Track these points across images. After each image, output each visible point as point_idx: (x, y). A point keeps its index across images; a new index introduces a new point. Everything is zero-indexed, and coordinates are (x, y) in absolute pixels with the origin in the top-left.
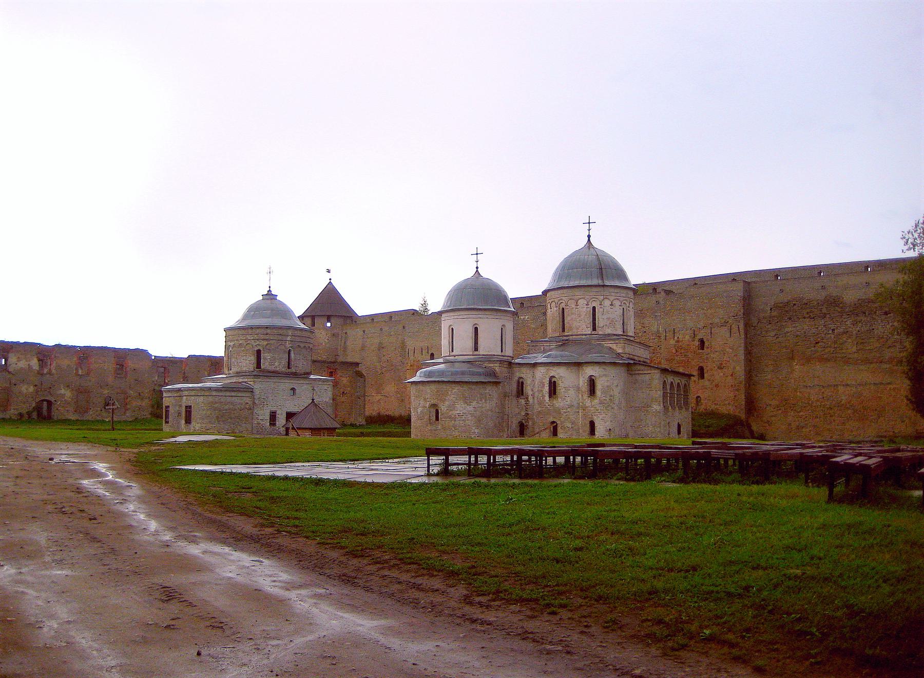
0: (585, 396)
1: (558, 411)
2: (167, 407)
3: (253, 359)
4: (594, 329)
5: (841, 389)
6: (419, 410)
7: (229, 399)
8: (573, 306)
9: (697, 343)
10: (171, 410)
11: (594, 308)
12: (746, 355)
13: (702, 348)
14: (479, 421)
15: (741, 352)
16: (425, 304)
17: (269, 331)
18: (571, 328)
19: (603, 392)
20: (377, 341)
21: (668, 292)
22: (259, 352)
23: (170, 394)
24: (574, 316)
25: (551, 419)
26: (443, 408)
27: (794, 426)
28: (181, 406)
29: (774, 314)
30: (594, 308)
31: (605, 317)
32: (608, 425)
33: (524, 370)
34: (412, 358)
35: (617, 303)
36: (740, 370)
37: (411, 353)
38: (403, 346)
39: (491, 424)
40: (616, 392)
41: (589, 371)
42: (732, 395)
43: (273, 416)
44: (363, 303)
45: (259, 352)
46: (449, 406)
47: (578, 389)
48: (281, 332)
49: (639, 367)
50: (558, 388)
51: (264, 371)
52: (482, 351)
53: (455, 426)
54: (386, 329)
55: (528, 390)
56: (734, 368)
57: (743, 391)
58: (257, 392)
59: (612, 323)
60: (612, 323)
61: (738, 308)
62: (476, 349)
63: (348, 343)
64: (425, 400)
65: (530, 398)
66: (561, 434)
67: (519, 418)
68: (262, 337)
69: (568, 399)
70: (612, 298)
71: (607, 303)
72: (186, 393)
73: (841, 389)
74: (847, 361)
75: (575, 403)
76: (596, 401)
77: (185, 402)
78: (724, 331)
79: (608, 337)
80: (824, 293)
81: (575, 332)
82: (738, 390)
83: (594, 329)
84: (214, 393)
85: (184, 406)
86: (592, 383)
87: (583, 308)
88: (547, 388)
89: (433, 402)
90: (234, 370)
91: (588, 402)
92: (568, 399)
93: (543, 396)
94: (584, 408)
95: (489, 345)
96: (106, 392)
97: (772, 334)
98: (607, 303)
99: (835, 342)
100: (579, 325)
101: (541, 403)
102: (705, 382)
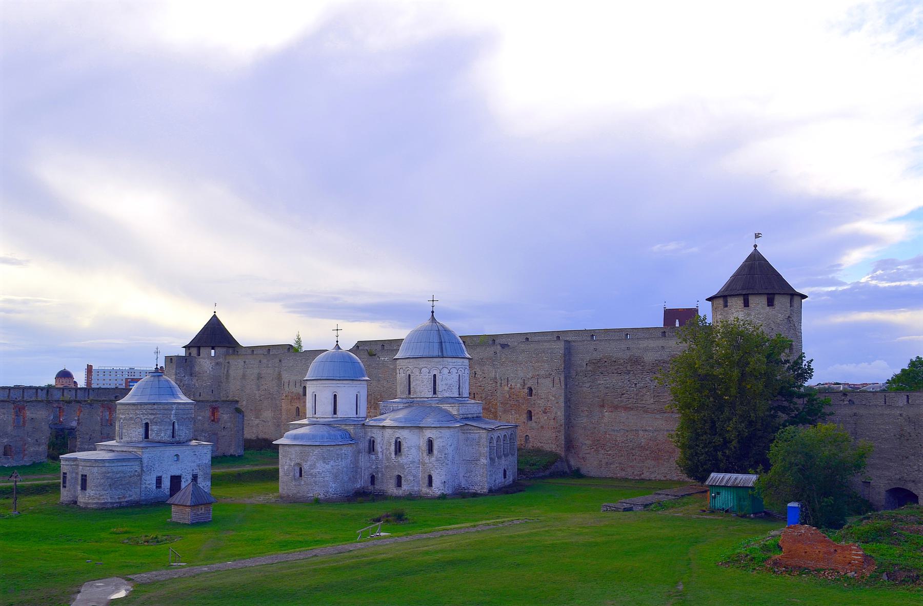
0: (425, 454)
1: (402, 466)
2: (65, 474)
3: (142, 430)
4: (435, 393)
5: (641, 433)
6: (286, 467)
7: (120, 469)
9: (526, 391)
10: (68, 476)
11: (435, 376)
12: (566, 403)
15: (562, 399)
16: (299, 341)
17: (155, 407)
18: (415, 392)
20: (256, 371)
21: (504, 346)
22: (147, 424)
23: (67, 463)
25: (397, 473)
26: (306, 467)
27: (604, 461)
28: (77, 473)
29: (589, 368)
30: (435, 376)
31: (444, 383)
32: (443, 478)
33: (375, 430)
34: (287, 389)
35: (454, 371)
36: (560, 414)
37: (286, 385)
38: (279, 377)
39: (346, 478)
40: (450, 450)
41: (428, 434)
42: (554, 435)
43: (159, 480)
44: (246, 330)
46: (311, 465)
48: (166, 407)
50: (402, 448)
51: (152, 442)
52: (340, 414)
53: (315, 482)
54: (264, 361)
55: (378, 447)
56: (556, 413)
57: (563, 432)
58: (145, 461)
59: (450, 387)
60: (450, 387)
61: (559, 363)
62: (335, 413)
63: (231, 372)
64: (290, 459)
65: (380, 455)
66: (405, 487)
67: (371, 471)
68: (151, 412)
70: (449, 367)
71: (446, 371)
72: (83, 463)
73: (641, 433)
74: (646, 412)
75: (416, 460)
77: (81, 470)
78: (548, 382)
79: (445, 400)
80: (628, 353)
81: (419, 395)
82: (559, 432)
83: (435, 393)
84: (107, 464)
85: (80, 474)
86: (430, 443)
87: (427, 378)
88: (393, 447)
89: (298, 461)
90: (125, 439)
91: (427, 459)
92: (411, 457)
93: (390, 454)
94: (424, 464)
95: (346, 409)
96: (6, 440)
97: (588, 385)
98: (446, 371)
99: (637, 395)
100: (422, 389)
101: (388, 459)
102: (532, 424)
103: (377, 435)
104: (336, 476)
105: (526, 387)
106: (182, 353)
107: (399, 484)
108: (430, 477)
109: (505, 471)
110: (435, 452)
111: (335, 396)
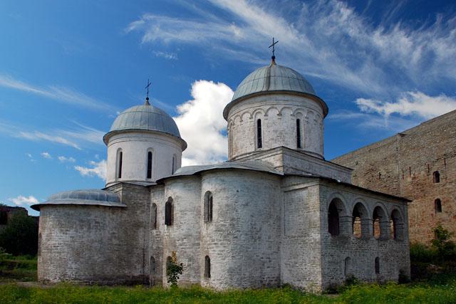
8: (239, 123)
9: (432, 176)
11: (259, 121)
13: (438, 181)
14: (78, 254)
19: (221, 215)
24: (239, 134)
31: (271, 129)
35: (288, 113)
39: (98, 258)
49: (293, 181)
59: (281, 135)
69: (184, 227)
70: (280, 107)
71: (273, 113)
76: (212, 227)
98: (273, 113)
104: (78, 254)
105: (432, 172)
108: (208, 259)
109: (377, 260)
110: (215, 215)
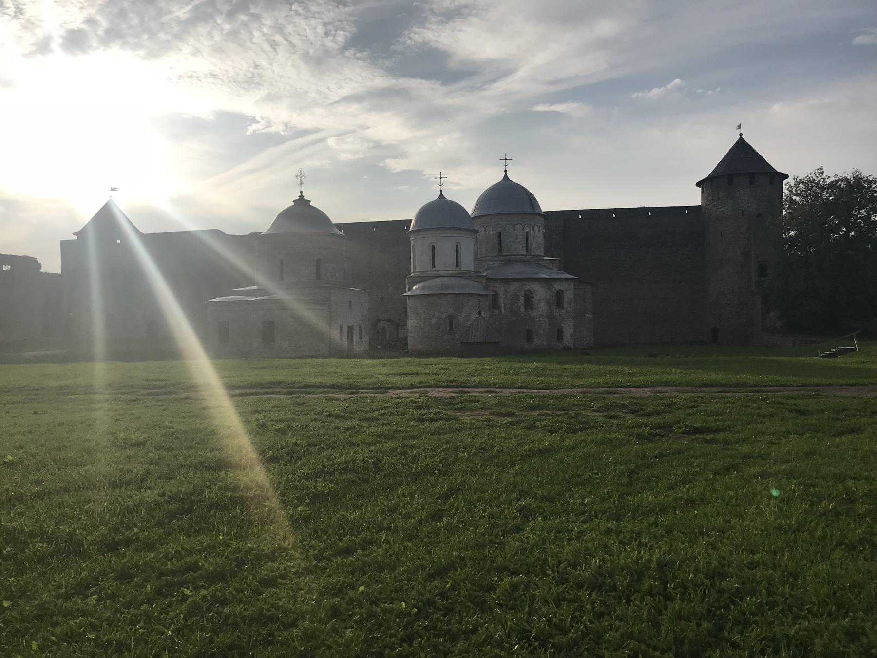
6: (434, 321)
45: (318, 262)
47: (547, 302)
65: (503, 309)
66: (536, 341)
88: (522, 301)
92: (540, 309)
93: (519, 308)
103: (500, 289)
106: (76, 238)
107: (529, 339)
110: (565, 305)
111: (457, 247)
